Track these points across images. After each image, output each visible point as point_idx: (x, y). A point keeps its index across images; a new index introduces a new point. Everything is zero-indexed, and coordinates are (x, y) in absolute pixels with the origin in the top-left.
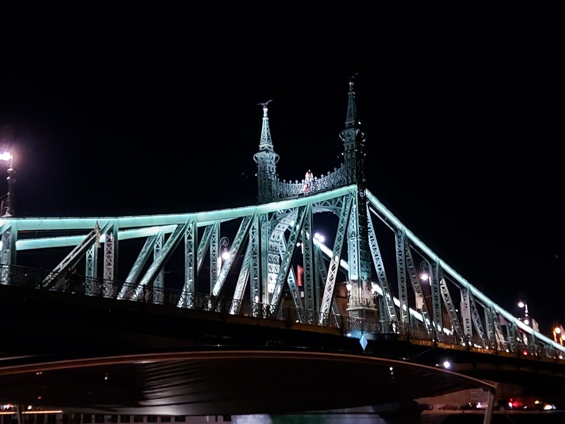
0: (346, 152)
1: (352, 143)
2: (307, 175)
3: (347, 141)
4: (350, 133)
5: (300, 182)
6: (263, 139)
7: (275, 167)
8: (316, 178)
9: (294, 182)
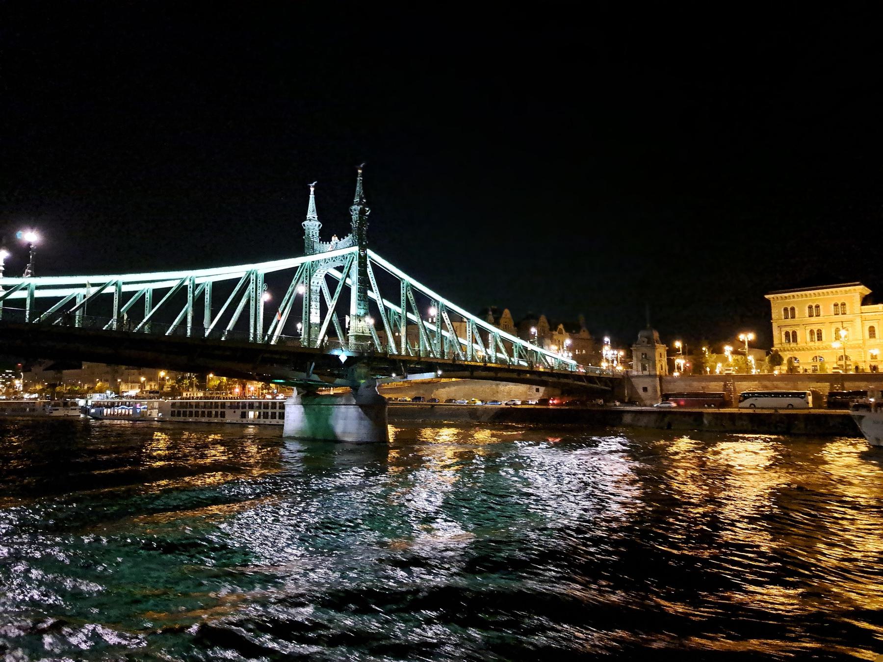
7: (318, 232)
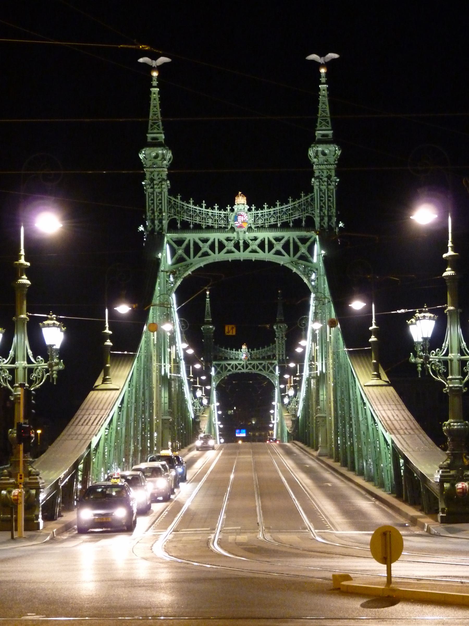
0: (318, 177)
1: (329, 167)
2: (241, 200)
3: (320, 162)
4: (327, 151)
6: (154, 123)
8: (253, 208)
9: (210, 205)
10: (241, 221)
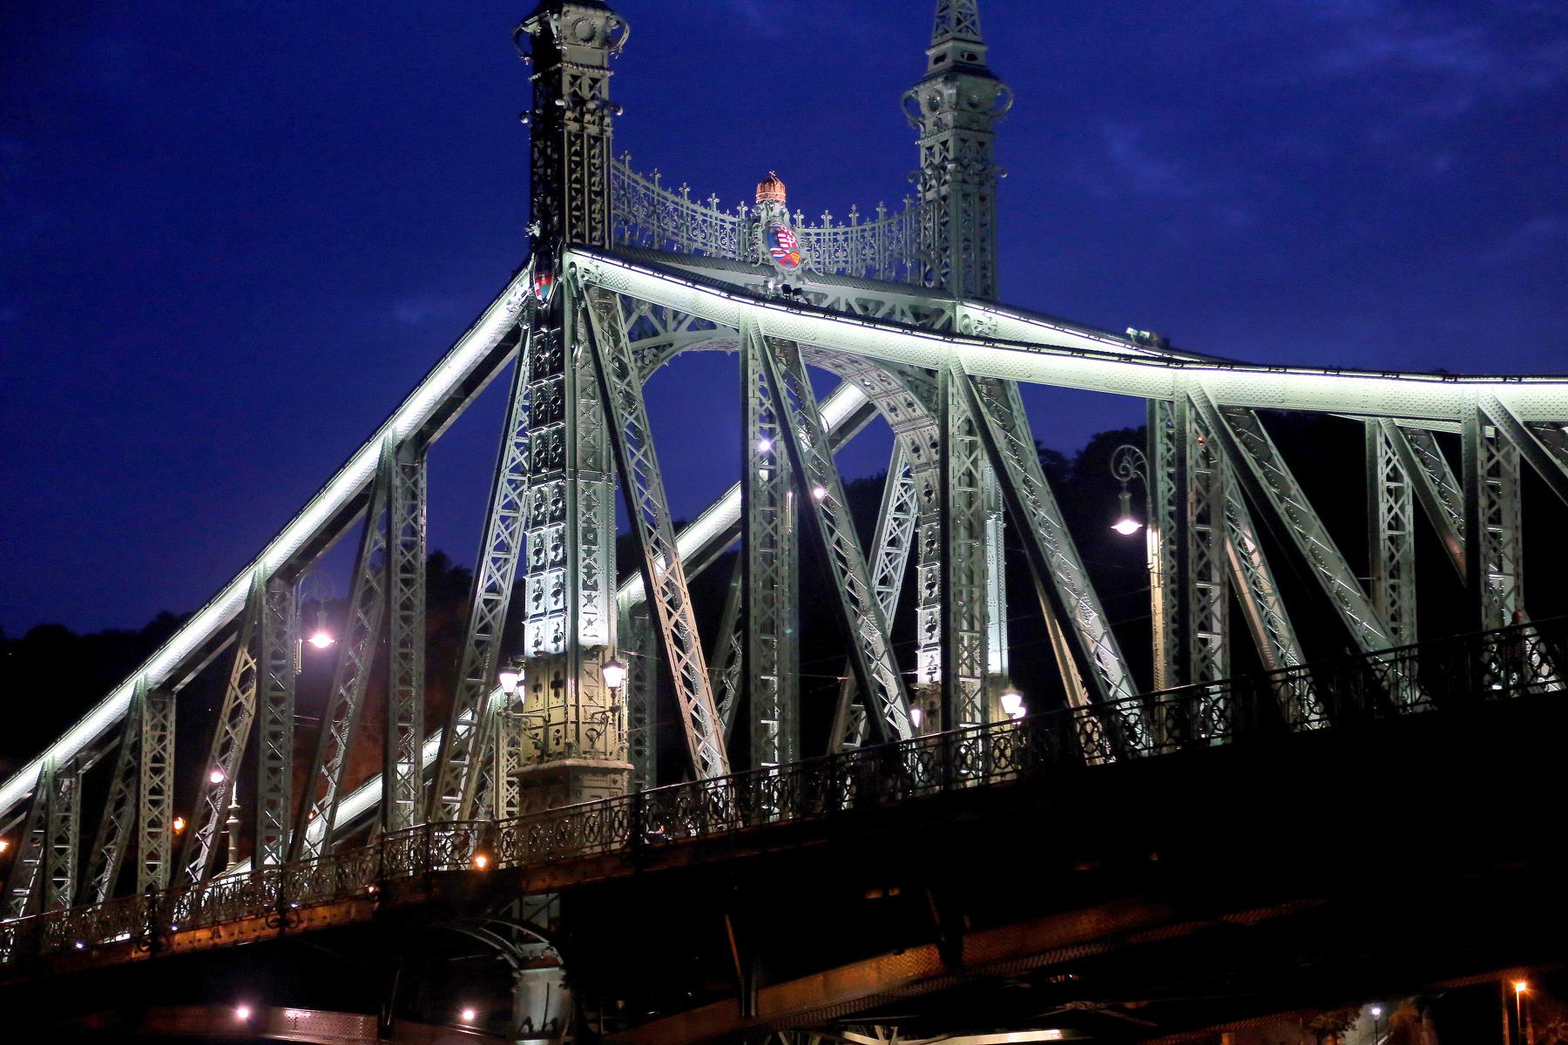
5: (727, 205)
8: (799, 217)
9: (699, 196)
10: (786, 246)
